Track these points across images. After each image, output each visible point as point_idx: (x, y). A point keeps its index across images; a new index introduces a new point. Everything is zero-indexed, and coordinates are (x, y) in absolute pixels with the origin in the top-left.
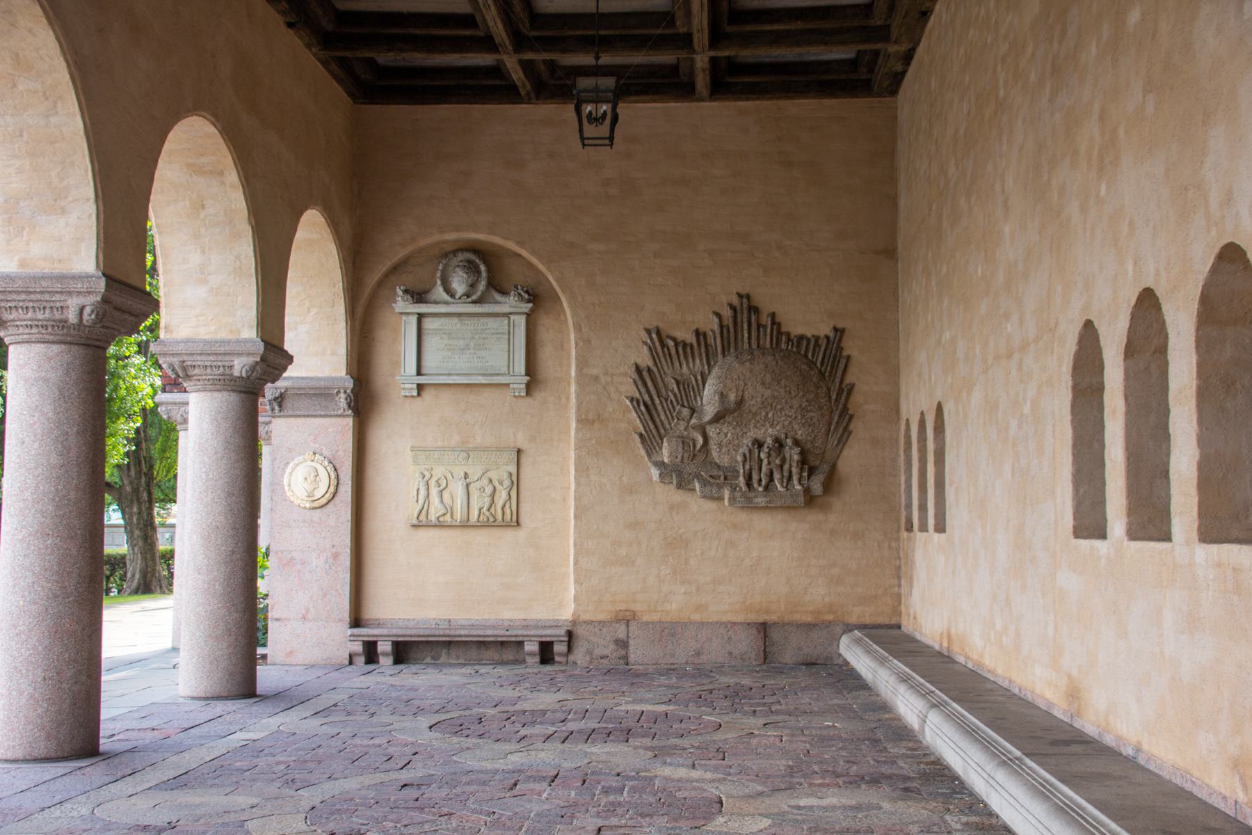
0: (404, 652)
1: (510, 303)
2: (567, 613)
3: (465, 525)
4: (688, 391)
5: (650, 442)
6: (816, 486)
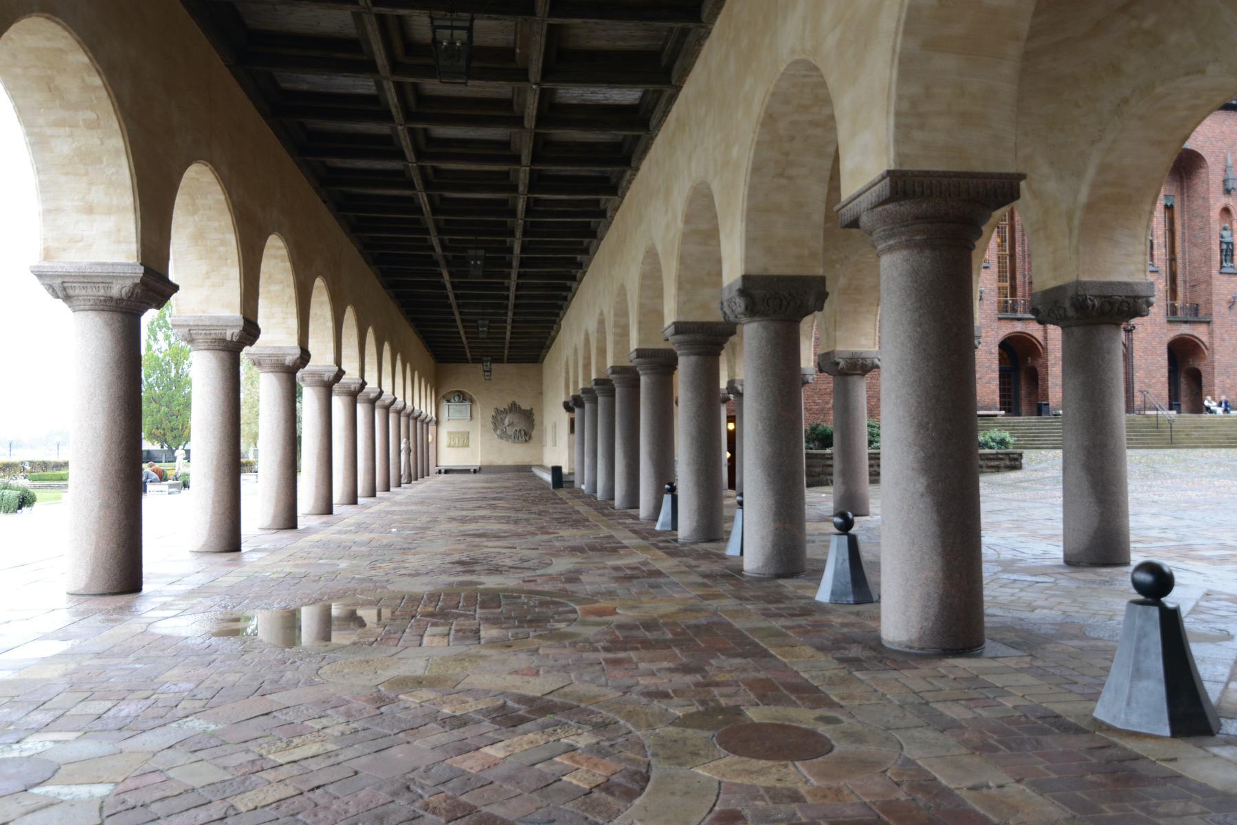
0: (447, 472)
1: (467, 403)
2: (479, 464)
3: (458, 447)
4: (502, 421)
5: (495, 430)
6: (527, 438)
